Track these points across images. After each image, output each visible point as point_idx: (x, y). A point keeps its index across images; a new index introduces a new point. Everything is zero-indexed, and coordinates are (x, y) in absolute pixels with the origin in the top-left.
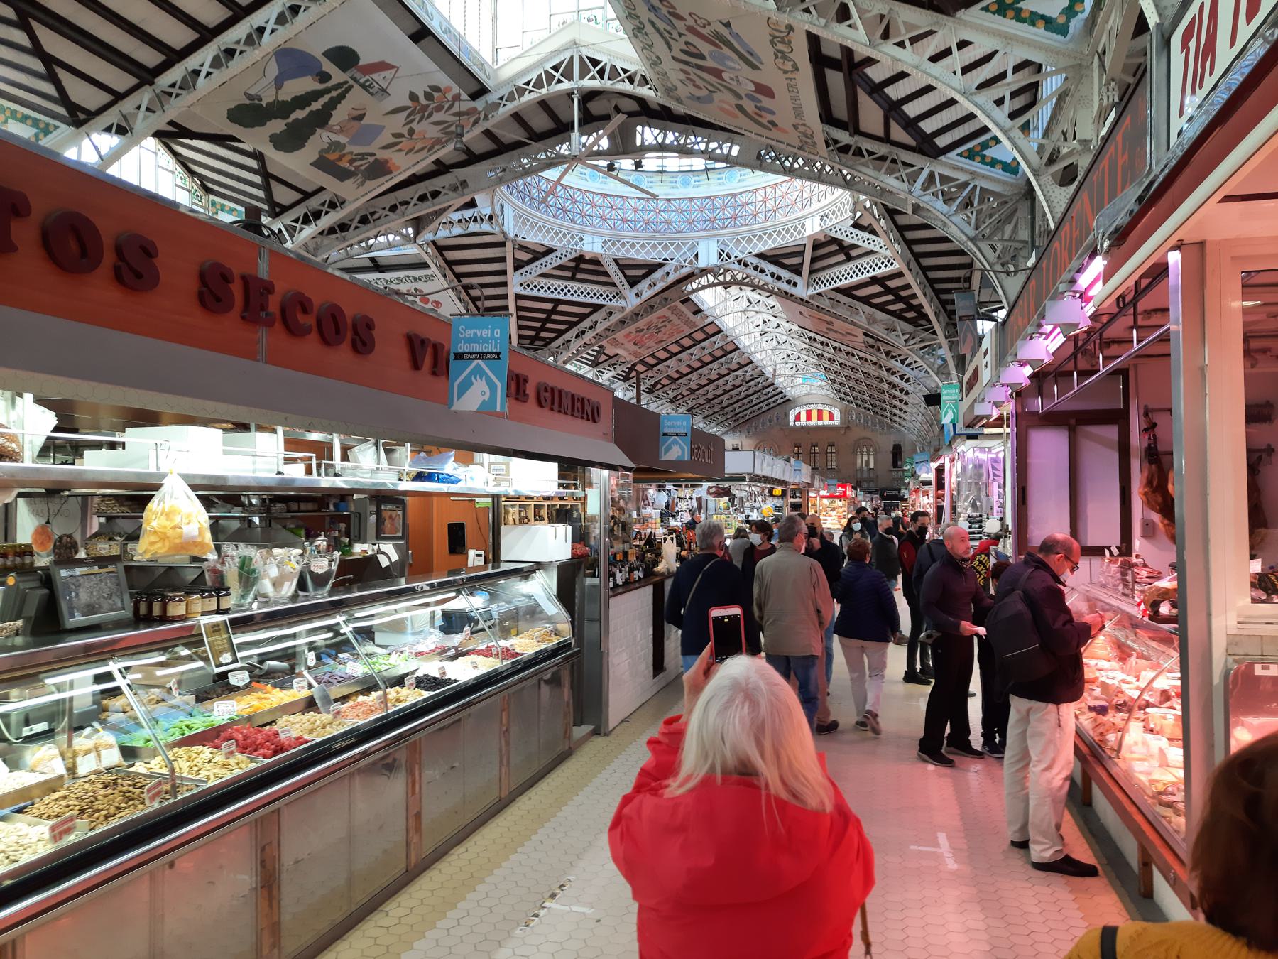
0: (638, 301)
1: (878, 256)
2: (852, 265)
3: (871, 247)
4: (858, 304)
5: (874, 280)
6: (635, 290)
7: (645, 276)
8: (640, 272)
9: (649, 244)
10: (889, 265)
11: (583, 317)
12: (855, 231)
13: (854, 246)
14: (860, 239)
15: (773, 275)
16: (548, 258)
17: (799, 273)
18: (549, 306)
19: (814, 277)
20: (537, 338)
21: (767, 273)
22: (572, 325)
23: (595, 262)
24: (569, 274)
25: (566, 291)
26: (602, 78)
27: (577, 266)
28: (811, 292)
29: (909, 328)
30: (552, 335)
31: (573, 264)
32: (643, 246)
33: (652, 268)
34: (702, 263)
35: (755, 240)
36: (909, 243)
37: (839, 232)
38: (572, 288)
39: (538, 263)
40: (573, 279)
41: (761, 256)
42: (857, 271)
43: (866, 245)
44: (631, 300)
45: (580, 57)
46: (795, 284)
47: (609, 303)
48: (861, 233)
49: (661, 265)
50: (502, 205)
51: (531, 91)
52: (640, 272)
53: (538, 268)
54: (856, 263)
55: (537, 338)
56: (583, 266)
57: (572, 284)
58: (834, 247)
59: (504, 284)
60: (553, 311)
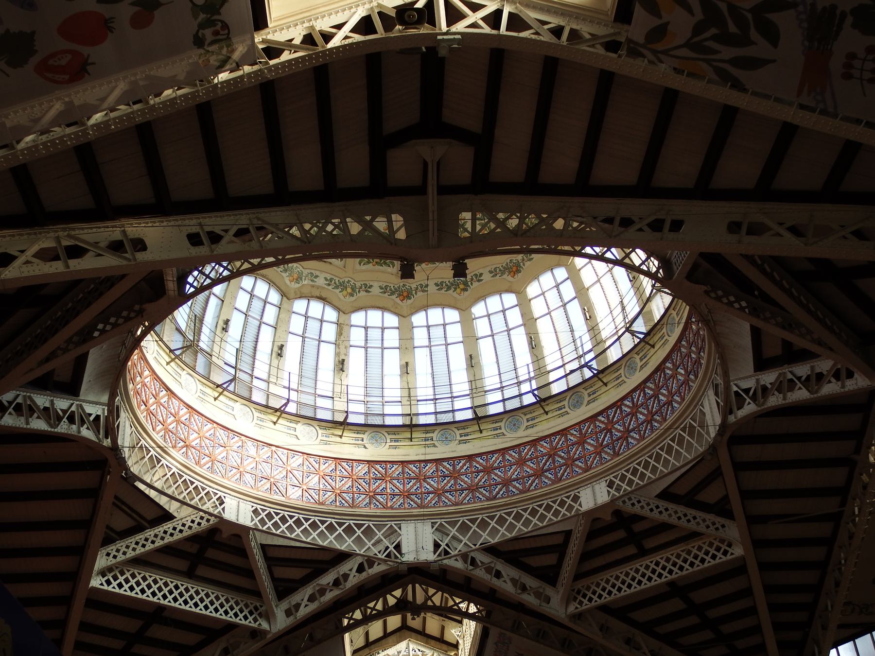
0: (291, 621)
3: (693, 526)
5: (674, 589)
6: (285, 605)
8: (296, 573)
9: (323, 522)
10: (708, 558)
12: (663, 504)
15: (514, 581)
18: (130, 625)
19: (579, 585)
24: (183, 565)
25: (176, 593)
28: (571, 609)
31: (194, 549)
34: (409, 556)
35: (493, 523)
36: (752, 520)
37: (638, 506)
39: (140, 537)
42: (659, 570)
43: (683, 522)
46: (548, 600)
48: (672, 506)
50: (118, 407)
52: (296, 573)
56: (211, 553)
58: (620, 534)
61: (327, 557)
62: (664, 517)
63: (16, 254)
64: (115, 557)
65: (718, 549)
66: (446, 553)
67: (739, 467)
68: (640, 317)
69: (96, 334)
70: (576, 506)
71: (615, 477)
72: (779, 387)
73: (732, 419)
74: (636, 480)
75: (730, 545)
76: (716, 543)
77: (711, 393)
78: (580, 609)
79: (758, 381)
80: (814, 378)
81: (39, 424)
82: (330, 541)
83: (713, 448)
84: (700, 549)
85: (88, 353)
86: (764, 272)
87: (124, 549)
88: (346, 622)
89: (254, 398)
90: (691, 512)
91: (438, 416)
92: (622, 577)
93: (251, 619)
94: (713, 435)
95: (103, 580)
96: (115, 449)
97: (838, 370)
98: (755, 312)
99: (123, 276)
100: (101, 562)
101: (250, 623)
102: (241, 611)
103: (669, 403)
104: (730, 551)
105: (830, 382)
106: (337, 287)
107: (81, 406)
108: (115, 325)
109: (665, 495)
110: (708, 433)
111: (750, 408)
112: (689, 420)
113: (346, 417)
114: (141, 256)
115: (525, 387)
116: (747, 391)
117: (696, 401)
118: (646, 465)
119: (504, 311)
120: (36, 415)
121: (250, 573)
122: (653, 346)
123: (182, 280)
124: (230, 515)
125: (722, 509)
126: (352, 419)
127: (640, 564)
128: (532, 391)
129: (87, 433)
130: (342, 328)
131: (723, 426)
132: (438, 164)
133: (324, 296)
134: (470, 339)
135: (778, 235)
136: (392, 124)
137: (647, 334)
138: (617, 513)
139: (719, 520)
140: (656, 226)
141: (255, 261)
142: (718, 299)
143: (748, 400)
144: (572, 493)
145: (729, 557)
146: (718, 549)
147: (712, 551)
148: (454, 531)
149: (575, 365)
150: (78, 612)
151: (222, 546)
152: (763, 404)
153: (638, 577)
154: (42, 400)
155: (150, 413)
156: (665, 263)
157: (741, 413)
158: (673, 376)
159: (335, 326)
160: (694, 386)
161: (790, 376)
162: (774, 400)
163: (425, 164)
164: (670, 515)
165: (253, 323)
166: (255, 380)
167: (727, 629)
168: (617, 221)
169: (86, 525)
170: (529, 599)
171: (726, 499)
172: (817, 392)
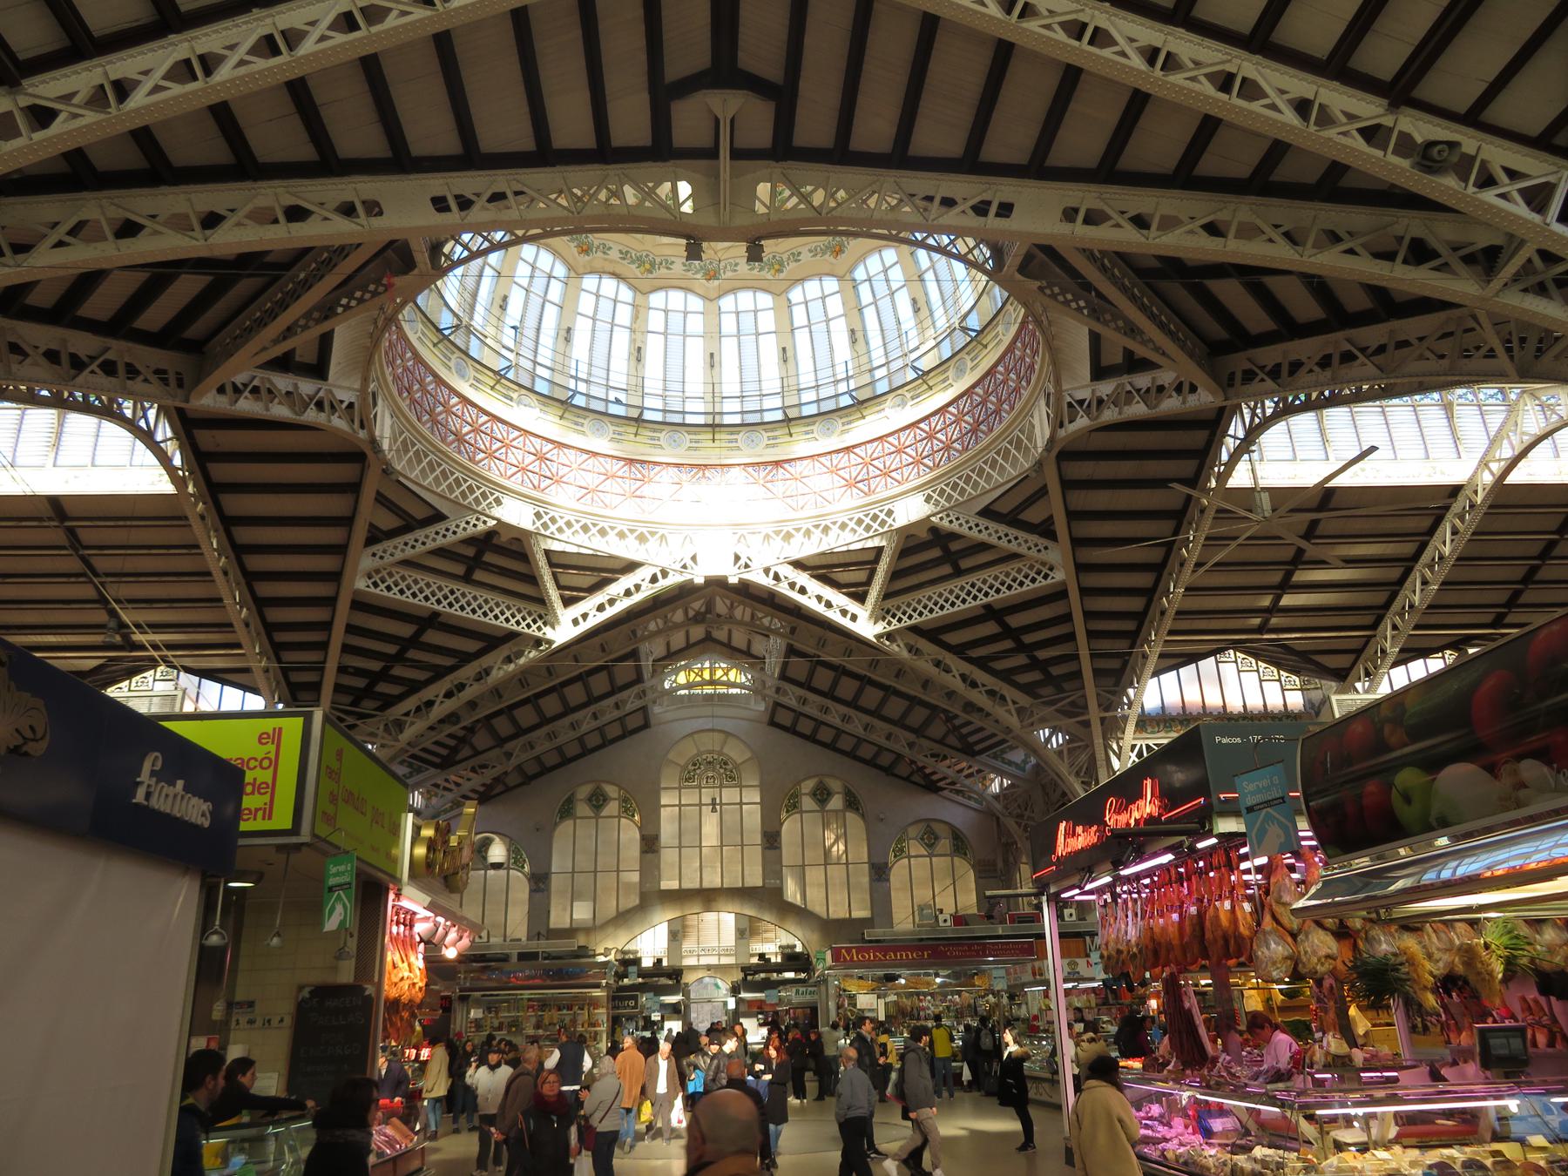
1: (1017, 565)
2: (961, 582)
3: (1013, 547)
4: (950, 659)
5: (990, 612)
11: (465, 658)
12: (983, 522)
14: (992, 532)
16: (430, 530)
18: (406, 630)
19: (889, 604)
20: (368, 692)
21: (810, 594)
22: (439, 673)
24: (460, 569)
25: (451, 598)
27: (479, 554)
28: (880, 627)
29: (1024, 700)
30: (395, 690)
31: (470, 552)
36: (1077, 542)
38: (463, 595)
39: (409, 537)
40: (467, 579)
42: (974, 592)
43: (1003, 543)
44: (565, 627)
46: (854, 618)
47: (526, 630)
48: (993, 526)
50: (374, 395)
53: (399, 549)
54: (972, 578)
55: (368, 692)
56: (489, 557)
57: (466, 589)
58: (936, 553)
59: (335, 577)
60: (414, 642)
61: (617, 566)
62: (984, 537)
63: (223, 212)
64: (381, 558)
65: (1038, 573)
66: (747, 566)
67: (1067, 485)
68: (974, 312)
69: (340, 310)
71: (934, 491)
72: (1118, 400)
73: (1062, 433)
74: (956, 495)
75: (1051, 569)
76: (1037, 566)
77: (1043, 402)
78: (889, 629)
79: (1093, 391)
80: (1154, 391)
81: (280, 411)
83: (1039, 465)
84: (1019, 571)
85: (333, 331)
86: (1103, 269)
87: (391, 550)
88: (639, 633)
89: (537, 389)
90: (1013, 532)
91: (745, 416)
92: (935, 597)
93: (534, 627)
94: (1040, 450)
95: (370, 582)
96: (374, 442)
97: (1181, 384)
98: (1095, 314)
99: (359, 245)
100: (366, 562)
102: (524, 619)
103: (997, 412)
104: (1051, 574)
105: (1170, 396)
106: (633, 262)
107: (331, 392)
108: (361, 301)
109: (987, 513)
110: (1035, 447)
111: (1082, 422)
112: (1017, 432)
113: (641, 414)
114: (376, 222)
115: (842, 387)
116: (1081, 402)
117: (1027, 412)
119: (823, 298)
120: (276, 400)
121: (533, 579)
122: (985, 346)
123: (436, 249)
125: (1046, 530)
126: (648, 415)
128: (849, 392)
129: (339, 422)
130: (638, 311)
131: (1052, 440)
132: (732, 121)
133: (618, 272)
134: (787, 329)
135: (1118, 225)
136: (674, 70)
137: (980, 333)
138: (934, 530)
139: (1042, 542)
140: (981, 209)
141: (520, 233)
142: (1054, 296)
143: (1081, 413)
144: (886, 508)
145: (1049, 581)
146: (1038, 573)
147: (1032, 574)
149: (899, 363)
150: (343, 614)
151: (502, 550)
152: (1097, 417)
153: (952, 598)
154: (282, 382)
155: (413, 401)
156: (998, 253)
157: (1072, 428)
158: (1005, 382)
159: (629, 308)
160: (1025, 394)
161: (1129, 388)
162: (1109, 415)
163: (717, 121)
164: (990, 535)
165: (535, 302)
166: (538, 367)
167: (1042, 654)
168: (937, 200)
169: (347, 521)
171: (1050, 520)
172: (1156, 406)
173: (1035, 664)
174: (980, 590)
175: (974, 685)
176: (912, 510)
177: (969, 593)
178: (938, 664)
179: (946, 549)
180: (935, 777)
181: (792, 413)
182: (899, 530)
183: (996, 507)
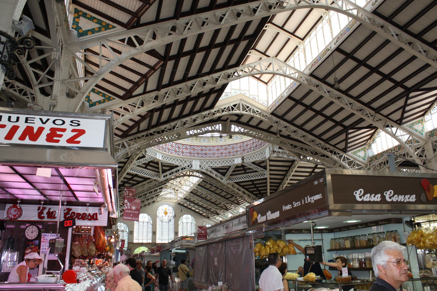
2: (247, 175)
3: (258, 170)
7: (169, 170)
9: (176, 159)
11: (139, 182)
12: (252, 165)
13: (250, 169)
14: (254, 167)
17: (224, 175)
19: (230, 177)
21: (214, 174)
22: (133, 185)
23: (157, 163)
24: (144, 166)
26: (250, 112)
28: (227, 182)
29: (254, 197)
31: (147, 163)
32: (174, 159)
33: (172, 167)
40: (146, 168)
41: (213, 169)
42: (248, 177)
45: (242, 104)
46: (222, 179)
48: (254, 165)
49: (177, 166)
51: (225, 111)
54: (248, 174)
56: (151, 164)
58: (242, 168)
60: (131, 179)
62: (252, 168)
70: (233, 162)
75: (264, 175)
82: (177, 163)
101: (155, 178)
109: (253, 163)
116: (275, 151)
118: (251, 157)
124: (157, 158)
125: (265, 168)
127: (245, 175)
139: (264, 170)
148: (205, 163)
170: (219, 179)
173: (258, 190)
174: (250, 177)
175: (245, 193)
176: (238, 161)
177: (247, 177)
178: (238, 189)
179: (244, 168)
180: (228, 208)
181: (213, 136)
182: (235, 165)
183: (255, 162)
